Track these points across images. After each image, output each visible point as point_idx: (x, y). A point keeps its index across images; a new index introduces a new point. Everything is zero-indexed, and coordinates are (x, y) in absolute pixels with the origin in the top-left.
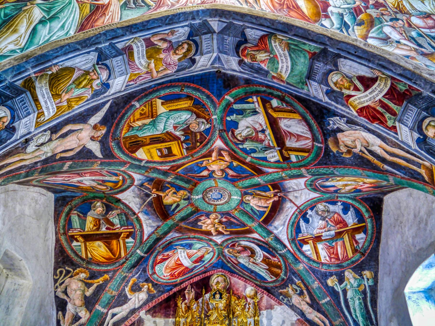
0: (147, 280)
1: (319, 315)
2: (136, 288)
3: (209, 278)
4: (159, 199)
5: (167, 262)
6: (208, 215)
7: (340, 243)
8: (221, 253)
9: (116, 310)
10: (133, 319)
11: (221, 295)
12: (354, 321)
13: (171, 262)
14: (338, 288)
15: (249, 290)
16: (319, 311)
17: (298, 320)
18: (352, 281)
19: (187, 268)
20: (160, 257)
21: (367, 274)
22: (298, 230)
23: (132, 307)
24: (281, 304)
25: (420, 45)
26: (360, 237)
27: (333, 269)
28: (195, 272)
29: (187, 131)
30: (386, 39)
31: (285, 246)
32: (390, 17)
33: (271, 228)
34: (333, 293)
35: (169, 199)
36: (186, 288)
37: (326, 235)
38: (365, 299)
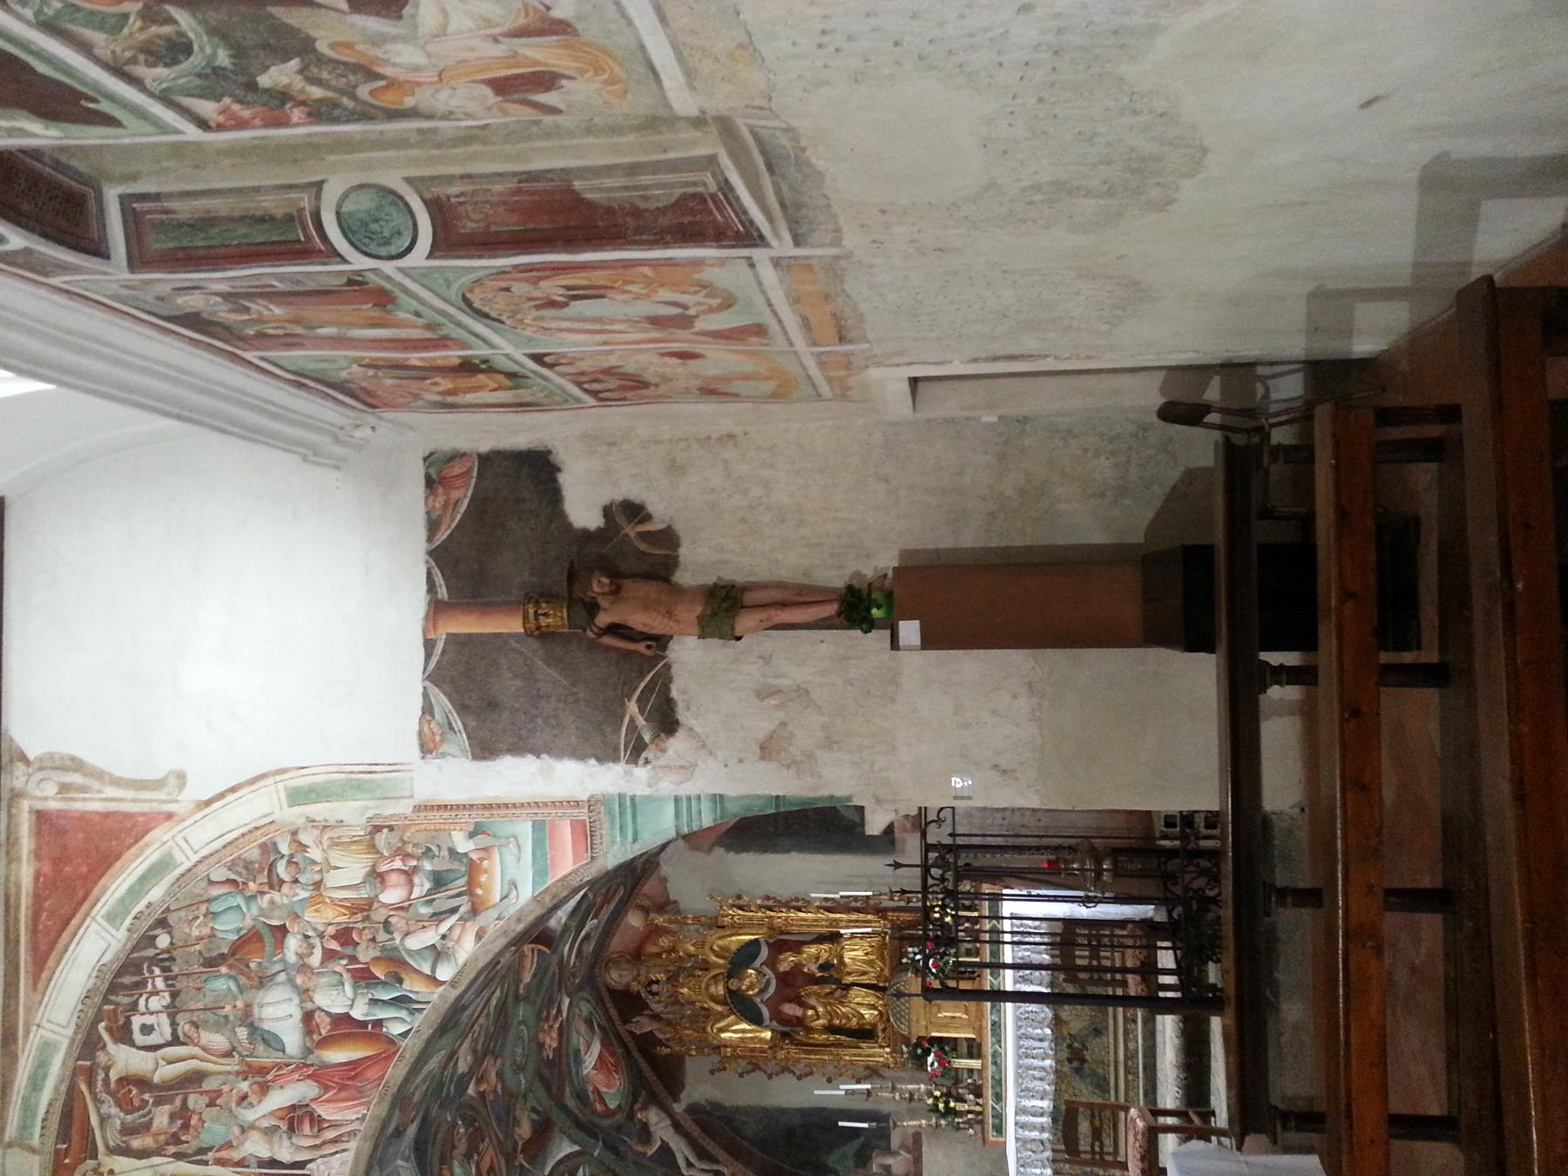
0: (631, 1116)
2: (645, 1134)
3: (612, 992)
4: (527, 1144)
5: (603, 1089)
6: (541, 1046)
8: (580, 989)
9: (681, 1163)
10: (688, 1124)
11: (652, 982)
13: (599, 1080)
15: (634, 920)
19: (602, 1044)
20: (599, 1107)
23: (671, 1130)
24: (658, 864)
25: (454, 911)
28: (604, 1023)
29: (468, 1156)
30: (437, 953)
31: (585, 895)
32: (381, 932)
33: (559, 929)
35: (524, 1131)
36: (631, 1033)
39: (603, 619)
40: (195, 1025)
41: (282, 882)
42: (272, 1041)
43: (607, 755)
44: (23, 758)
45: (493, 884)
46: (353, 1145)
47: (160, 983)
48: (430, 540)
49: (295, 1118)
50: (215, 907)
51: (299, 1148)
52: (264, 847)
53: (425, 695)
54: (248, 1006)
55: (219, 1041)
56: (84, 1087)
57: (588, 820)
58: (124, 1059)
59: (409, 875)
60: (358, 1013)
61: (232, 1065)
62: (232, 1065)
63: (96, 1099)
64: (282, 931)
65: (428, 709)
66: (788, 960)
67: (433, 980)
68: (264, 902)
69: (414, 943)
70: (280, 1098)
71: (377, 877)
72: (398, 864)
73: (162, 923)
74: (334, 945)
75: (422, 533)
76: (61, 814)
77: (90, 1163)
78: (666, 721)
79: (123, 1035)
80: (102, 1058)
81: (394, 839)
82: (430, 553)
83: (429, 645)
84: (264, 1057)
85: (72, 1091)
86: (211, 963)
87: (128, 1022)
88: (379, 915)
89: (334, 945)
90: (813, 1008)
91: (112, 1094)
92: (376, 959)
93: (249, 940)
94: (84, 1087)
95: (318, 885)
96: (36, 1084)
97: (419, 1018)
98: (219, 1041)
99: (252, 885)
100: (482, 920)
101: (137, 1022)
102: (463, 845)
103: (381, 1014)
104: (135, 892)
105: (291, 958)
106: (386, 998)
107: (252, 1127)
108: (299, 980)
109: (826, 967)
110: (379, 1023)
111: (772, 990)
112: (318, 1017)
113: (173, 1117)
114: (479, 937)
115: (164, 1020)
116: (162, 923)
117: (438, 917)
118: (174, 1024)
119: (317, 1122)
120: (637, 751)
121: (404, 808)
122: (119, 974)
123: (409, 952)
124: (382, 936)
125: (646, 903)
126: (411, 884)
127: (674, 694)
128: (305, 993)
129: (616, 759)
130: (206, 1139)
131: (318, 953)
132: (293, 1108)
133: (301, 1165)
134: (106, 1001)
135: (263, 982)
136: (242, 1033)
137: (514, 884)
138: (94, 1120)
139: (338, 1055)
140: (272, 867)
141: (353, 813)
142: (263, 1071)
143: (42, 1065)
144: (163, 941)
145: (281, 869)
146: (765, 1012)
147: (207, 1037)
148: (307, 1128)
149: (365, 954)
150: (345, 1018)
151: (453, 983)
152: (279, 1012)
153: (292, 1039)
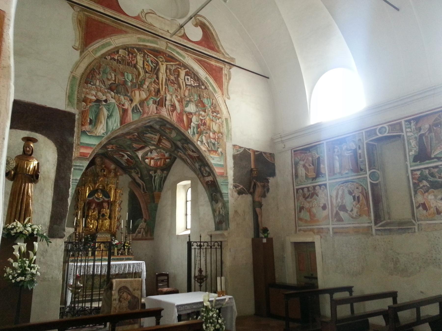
1: (142, 182)
7: (160, 161)
11: (104, 170)
12: (155, 186)
14: (153, 175)
15: (113, 166)
16: (143, 181)
17: (132, 181)
18: (159, 173)
21: (165, 172)
22: (147, 155)
26: (168, 160)
27: (153, 169)
30: (202, 142)
31: (139, 158)
34: (151, 176)
37: (156, 158)
38: (161, 180)
39: (258, 184)
40: (189, 90)
41: (213, 113)
42: (187, 105)
43: (235, 180)
44: (230, 69)
45: (213, 155)
46: (169, 118)
47: (196, 84)
48: (263, 152)
49: (173, 106)
50: (209, 99)
51: (168, 106)
52: (218, 111)
53: (242, 147)
54: (193, 102)
55: (187, 94)
56: (177, 63)
57: (224, 175)
58: (183, 73)
59: (215, 139)
60: (192, 124)
61: (183, 96)
62: (183, 96)
63: (175, 65)
64: (205, 112)
65: (240, 147)
66: (105, 205)
67: (198, 140)
68: (210, 109)
69: (204, 137)
70: (177, 104)
71: (214, 133)
72: (217, 137)
73: (206, 88)
74: (203, 122)
75: (264, 151)
76: (222, 73)
77: (164, 60)
78: (240, 193)
79: (187, 74)
80: (183, 68)
81: (220, 137)
82: (261, 152)
83: (249, 149)
84: (184, 103)
85: (178, 61)
86: (199, 96)
87: (189, 76)
88: (208, 132)
89: (203, 122)
90: (93, 212)
91: (176, 69)
92: (201, 129)
93: (204, 106)
94: (177, 63)
95: (213, 121)
96: (178, 53)
97: (191, 136)
98: (187, 94)
99: (212, 108)
100: (207, 152)
101: (189, 77)
102: (220, 150)
103: (192, 128)
104: (210, 84)
105: (201, 112)
106: (195, 130)
107: (172, 97)
108: (197, 113)
109: (103, 215)
110: (190, 128)
111: (97, 201)
112: (191, 116)
113: (173, 80)
114: (205, 151)
115: (189, 84)
116: (206, 88)
117: (208, 143)
118: (189, 85)
119: (173, 111)
120: (235, 186)
121: (225, 140)
122: (197, 76)
123: (202, 137)
124: (205, 131)
125: (117, 170)
126: (213, 139)
127: (243, 195)
128: (195, 114)
129: (234, 182)
130: (170, 86)
131: (202, 118)
132: (175, 107)
133: (165, 106)
134: (192, 72)
135: (197, 106)
136: (188, 99)
137: (213, 159)
138: (172, 63)
139: (185, 118)
140: (215, 112)
141: (224, 130)
142: (182, 102)
143: (181, 55)
144: (203, 87)
145: (215, 114)
146: (91, 198)
147: (187, 91)
148: (172, 109)
149: (202, 127)
150: (191, 122)
151: (197, 144)
152: (191, 108)
153: (187, 109)
